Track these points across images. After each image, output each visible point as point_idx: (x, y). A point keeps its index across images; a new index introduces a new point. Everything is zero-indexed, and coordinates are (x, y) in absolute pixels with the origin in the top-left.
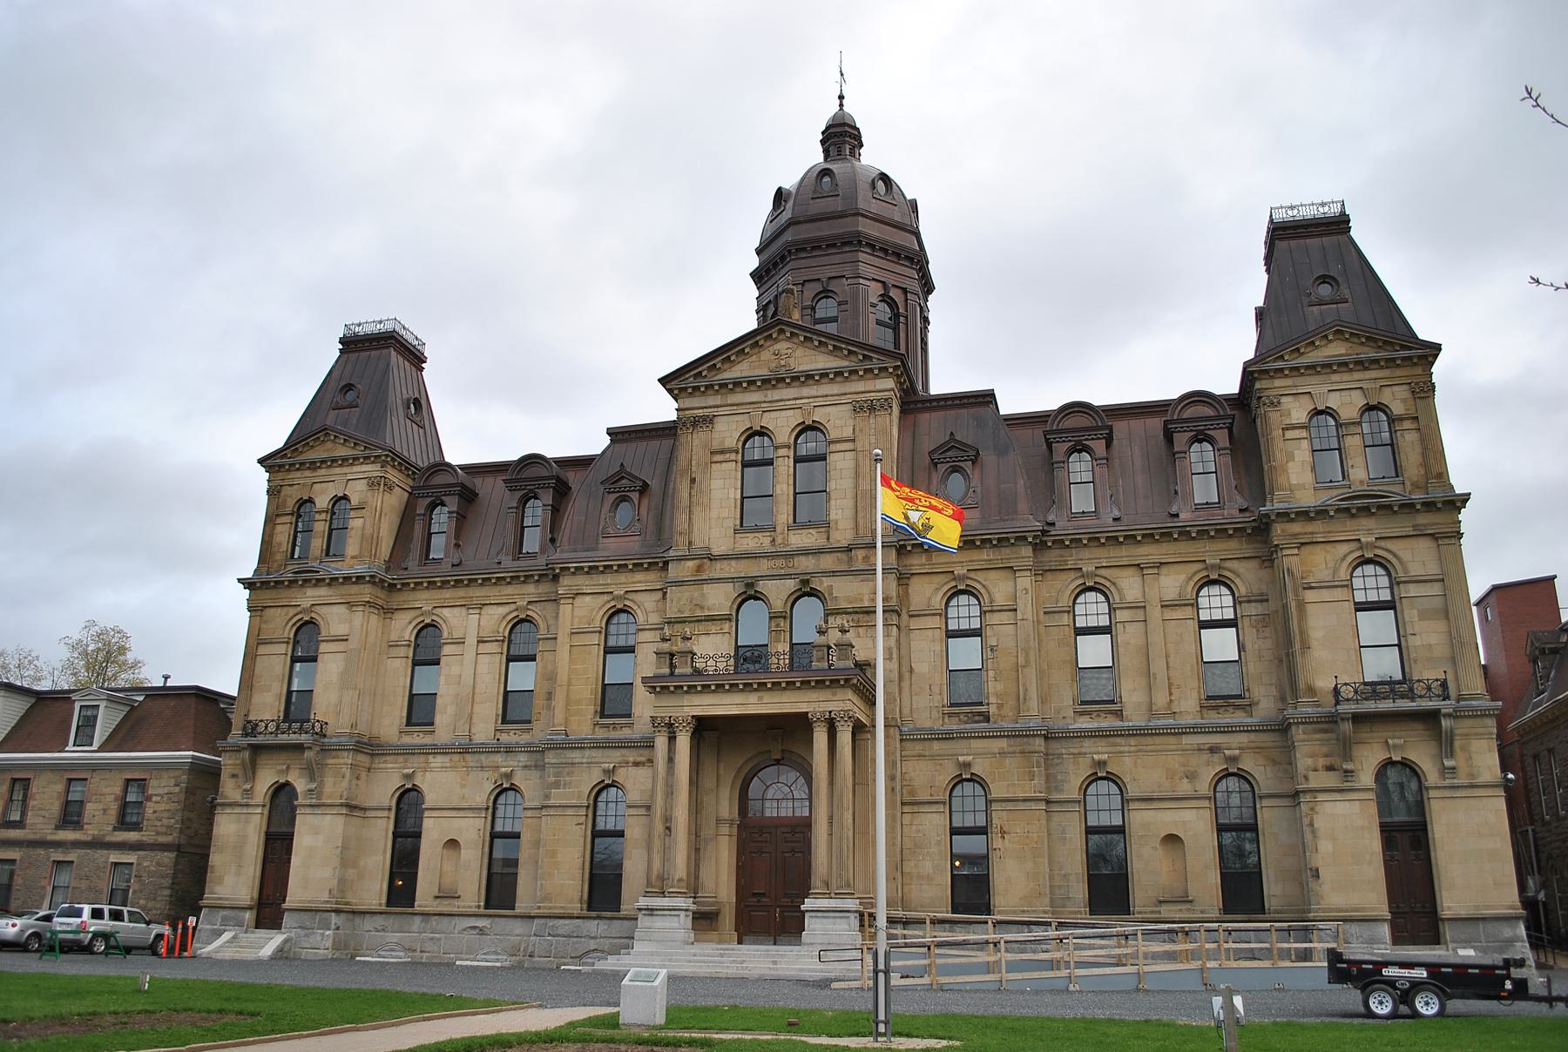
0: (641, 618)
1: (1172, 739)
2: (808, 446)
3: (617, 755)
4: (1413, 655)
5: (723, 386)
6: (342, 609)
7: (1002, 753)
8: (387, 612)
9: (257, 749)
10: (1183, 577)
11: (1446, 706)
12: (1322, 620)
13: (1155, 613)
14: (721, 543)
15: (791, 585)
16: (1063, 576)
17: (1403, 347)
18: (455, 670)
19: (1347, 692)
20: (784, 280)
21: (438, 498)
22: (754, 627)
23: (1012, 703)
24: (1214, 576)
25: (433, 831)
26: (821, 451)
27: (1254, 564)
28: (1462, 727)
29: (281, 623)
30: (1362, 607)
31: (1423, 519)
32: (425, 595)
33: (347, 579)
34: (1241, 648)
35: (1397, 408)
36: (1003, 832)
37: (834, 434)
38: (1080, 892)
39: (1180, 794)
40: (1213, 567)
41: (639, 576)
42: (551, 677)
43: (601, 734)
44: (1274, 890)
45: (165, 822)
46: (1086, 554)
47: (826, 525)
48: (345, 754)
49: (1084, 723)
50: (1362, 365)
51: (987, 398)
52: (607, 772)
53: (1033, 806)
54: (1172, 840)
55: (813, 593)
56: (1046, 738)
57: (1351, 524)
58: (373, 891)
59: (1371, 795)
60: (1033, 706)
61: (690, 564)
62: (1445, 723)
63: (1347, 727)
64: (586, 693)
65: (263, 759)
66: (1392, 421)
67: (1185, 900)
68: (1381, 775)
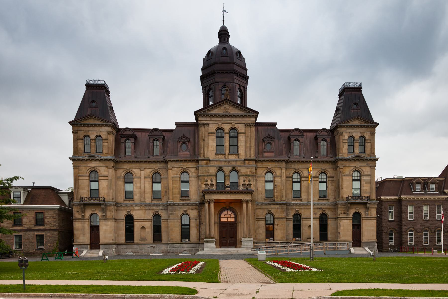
2: (233, 134)
3: (187, 207)
5: (211, 115)
6: (105, 168)
7: (277, 208)
8: (116, 169)
9: (85, 205)
11: (369, 202)
15: (230, 168)
16: (291, 169)
17: (371, 123)
18: (138, 185)
19: (350, 198)
21: (128, 138)
22: (221, 178)
23: (279, 197)
25: (137, 225)
26: (236, 135)
28: (371, 206)
29: (84, 170)
30: (354, 180)
31: (369, 163)
32: (127, 165)
33: (106, 160)
35: (367, 137)
36: (277, 225)
37: (240, 131)
41: (190, 164)
42: (167, 188)
43: (182, 202)
45: (52, 224)
46: (296, 165)
47: (238, 154)
50: (361, 126)
51: (275, 124)
52: (185, 211)
53: (284, 219)
55: (236, 171)
56: (287, 205)
57: (354, 163)
58: (122, 239)
59: (352, 219)
61: (205, 162)
63: (349, 205)
64: (177, 192)
68: (354, 215)
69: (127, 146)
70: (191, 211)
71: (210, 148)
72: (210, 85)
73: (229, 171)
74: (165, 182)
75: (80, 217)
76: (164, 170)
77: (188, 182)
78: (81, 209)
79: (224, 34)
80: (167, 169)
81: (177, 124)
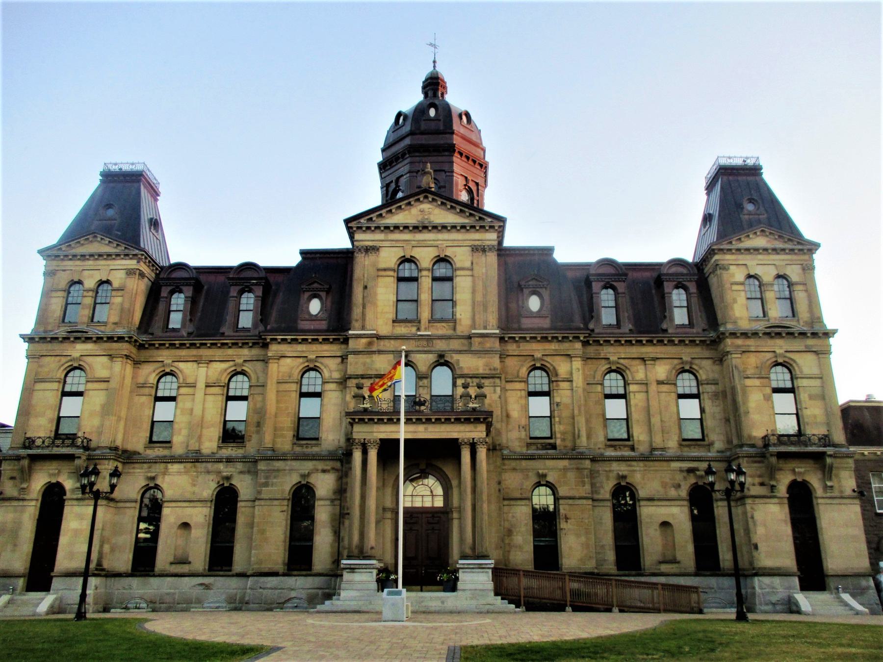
0: (326, 374)
1: (665, 464)
2: (442, 270)
3: (309, 465)
4: (806, 420)
5: (387, 228)
6: (105, 359)
7: (565, 469)
8: (137, 363)
9: (34, 458)
10: (668, 367)
11: (830, 450)
12: (753, 399)
13: (653, 387)
14: (385, 329)
15: (432, 358)
17: (799, 243)
18: (188, 405)
20: (403, 168)
23: (569, 437)
24: (687, 367)
25: (170, 516)
26: (449, 274)
27: (709, 362)
28: (836, 462)
29: (53, 366)
30: (777, 390)
31: (811, 342)
33: (110, 339)
34: (702, 411)
35: (794, 278)
38: (610, 556)
39: (669, 497)
40: (687, 362)
44: (725, 556)
46: (611, 349)
47: (453, 321)
48: (106, 462)
49: (610, 453)
50: (775, 250)
51: (549, 251)
52: (303, 476)
53: (584, 502)
54: (665, 524)
55: (446, 364)
56: (593, 460)
57: (770, 342)
59: (786, 501)
60: (584, 439)
61: (364, 341)
62: (829, 460)
63: (774, 460)
64: (287, 423)
65: (38, 466)
66: (790, 285)
67: (674, 561)
69: (173, 308)
70: (321, 476)
71: (378, 303)
72: (398, 179)
73: (428, 364)
74: (259, 398)
75: (15, 493)
76: (259, 365)
77: (318, 395)
78: (22, 470)
79: (433, 85)
80: (265, 361)
81: (304, 253)
